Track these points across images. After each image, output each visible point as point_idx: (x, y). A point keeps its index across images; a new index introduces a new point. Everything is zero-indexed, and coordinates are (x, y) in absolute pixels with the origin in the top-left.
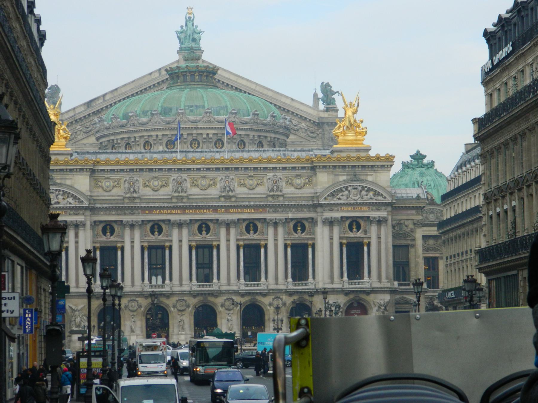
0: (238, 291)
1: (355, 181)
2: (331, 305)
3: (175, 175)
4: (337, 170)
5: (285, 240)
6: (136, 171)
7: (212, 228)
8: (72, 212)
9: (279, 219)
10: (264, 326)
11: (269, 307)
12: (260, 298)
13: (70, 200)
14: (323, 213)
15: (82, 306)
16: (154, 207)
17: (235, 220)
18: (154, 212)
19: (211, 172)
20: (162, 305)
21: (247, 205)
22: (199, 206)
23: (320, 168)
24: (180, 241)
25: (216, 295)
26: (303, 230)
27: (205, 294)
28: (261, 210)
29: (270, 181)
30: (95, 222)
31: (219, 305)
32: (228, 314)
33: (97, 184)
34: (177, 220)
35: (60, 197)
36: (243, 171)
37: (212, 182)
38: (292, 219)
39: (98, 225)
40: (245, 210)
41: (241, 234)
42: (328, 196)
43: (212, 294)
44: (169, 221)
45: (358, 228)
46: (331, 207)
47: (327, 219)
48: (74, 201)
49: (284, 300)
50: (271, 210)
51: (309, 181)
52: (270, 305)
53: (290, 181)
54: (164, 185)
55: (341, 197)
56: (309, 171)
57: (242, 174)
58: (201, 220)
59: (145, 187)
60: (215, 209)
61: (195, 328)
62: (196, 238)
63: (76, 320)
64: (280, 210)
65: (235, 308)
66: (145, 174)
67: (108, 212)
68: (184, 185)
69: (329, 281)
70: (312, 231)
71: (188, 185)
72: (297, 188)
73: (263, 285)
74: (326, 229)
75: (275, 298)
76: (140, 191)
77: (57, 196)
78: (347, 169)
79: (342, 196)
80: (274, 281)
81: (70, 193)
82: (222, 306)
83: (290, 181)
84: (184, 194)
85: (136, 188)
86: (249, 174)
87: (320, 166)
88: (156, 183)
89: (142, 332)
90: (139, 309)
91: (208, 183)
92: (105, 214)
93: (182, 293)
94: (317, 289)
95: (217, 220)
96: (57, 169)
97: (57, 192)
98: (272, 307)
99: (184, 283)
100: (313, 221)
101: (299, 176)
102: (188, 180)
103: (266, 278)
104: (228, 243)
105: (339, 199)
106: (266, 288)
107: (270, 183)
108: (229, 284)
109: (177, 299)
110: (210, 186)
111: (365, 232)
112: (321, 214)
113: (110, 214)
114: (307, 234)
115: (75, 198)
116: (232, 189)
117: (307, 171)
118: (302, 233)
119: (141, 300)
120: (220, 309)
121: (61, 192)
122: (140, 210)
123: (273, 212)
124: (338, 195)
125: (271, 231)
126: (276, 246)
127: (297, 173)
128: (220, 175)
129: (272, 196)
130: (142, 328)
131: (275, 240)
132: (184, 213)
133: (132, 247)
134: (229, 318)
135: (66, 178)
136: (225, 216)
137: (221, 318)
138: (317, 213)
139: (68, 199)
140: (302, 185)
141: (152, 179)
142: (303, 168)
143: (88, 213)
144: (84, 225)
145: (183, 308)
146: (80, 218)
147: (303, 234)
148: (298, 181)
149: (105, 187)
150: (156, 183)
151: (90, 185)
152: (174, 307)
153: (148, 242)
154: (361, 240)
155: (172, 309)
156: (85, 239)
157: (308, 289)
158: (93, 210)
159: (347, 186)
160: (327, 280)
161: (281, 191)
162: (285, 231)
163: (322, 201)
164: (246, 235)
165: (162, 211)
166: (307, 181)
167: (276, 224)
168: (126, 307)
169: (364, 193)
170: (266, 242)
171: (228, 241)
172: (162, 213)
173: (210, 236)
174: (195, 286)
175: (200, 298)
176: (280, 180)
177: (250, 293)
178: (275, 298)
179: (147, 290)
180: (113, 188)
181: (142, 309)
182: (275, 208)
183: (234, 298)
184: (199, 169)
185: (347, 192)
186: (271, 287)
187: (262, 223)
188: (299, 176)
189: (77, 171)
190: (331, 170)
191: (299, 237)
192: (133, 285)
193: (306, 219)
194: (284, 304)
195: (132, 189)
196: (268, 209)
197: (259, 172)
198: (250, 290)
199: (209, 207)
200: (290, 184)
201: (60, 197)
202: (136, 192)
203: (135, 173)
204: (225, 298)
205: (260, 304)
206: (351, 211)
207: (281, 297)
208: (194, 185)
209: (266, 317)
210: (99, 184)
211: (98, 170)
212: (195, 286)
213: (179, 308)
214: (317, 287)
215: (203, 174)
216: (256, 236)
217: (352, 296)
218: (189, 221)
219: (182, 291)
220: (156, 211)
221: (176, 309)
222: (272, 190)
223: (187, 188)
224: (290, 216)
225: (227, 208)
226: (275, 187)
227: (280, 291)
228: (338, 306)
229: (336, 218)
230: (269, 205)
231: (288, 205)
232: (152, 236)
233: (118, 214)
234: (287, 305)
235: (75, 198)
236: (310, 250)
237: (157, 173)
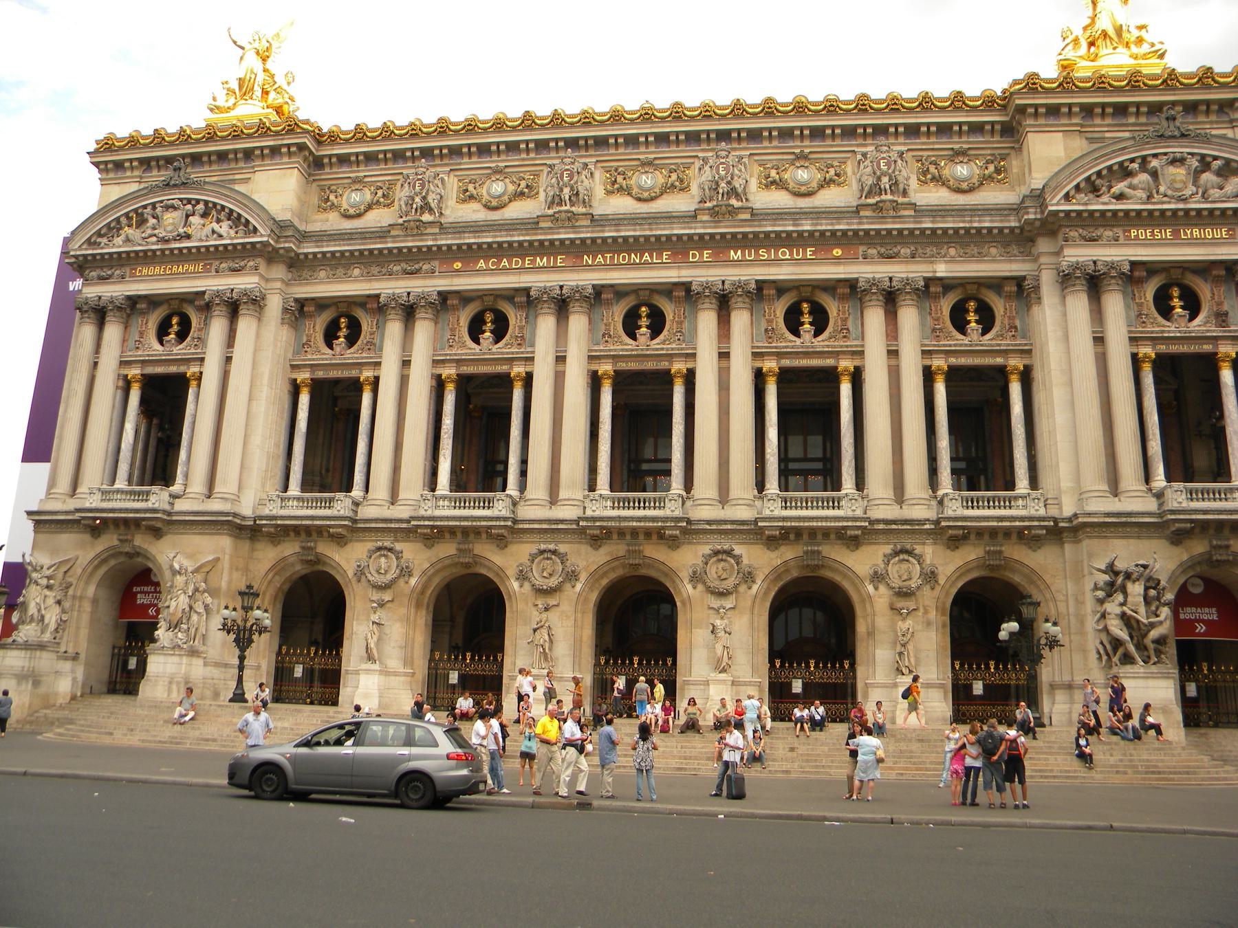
0: (756, 521)
1: (1173, 137)
2: (1128, 576)
3: (552, 159)
4: (1098, 121)
5: (926, 353)
6: (441, 156)
7: (669, 317)
8: (223, 265)
9: (902, 280)
10: (853, 665)
11: (870, 588)
12: (836, 553)
13: (224, 228)
14: (1062, 248)
15: (210, 558)
16: (480, 245)
17: (747, 283)
18: (482, 264)
19: (674, 148)
20: (483, 571)
21: (789, 234)
22: (625, 238)
23: (1036, 115)
24: (561, 359)
25: (674, 538)
26: (987, 321)
27: (634, 532)
28: (837, 252)
29: (867, 162)
30: (301, 303)
31: (685, 575)
32: (717, 611)
33: (328, 200)
34: (552, 289)
35: (195, 220)
36: (775, 143)
37: (674, 176)
38: (947, 285)
39: (311, 316)
40: (783, 253)
41: (769, 333)
42: (1077, 187)
43: (657, 534)
44: (527, 291)
45: (1193, 307)
46: (1092, 224)
47: (1076, 266)
48: (232, 232)
49: (928, 562)
50: (873, 251)
51: (998, 171)
52: (878, 578)
53: (932, 169)
54: (522, 194)
55: (1128, 191)
56: (997, 138)
57: (771, 150)
58: (635, 289)
59: (464, 201)
60: (680, 247)
61: (597, 656)
62: (614, 348)
63: (173, 604)
64: (905, 251)
65: (743, 588)
66: (466, 162)
67: (340, 271)
68: (584, 184)
69: (1106, 487)
70: (1018, 323)
71: (599, 191)
72: (959, 191)
73: (848, 506)
74: (1079, 304)
75: (896, 553)
76: (447, 212)
77: (187, 216)
78: (1132, 120)
79: (1131, 187)
80: (890, 493)
81: (223, 207)
82: (696, 578)
83: (932, 169)
84: (581, 209)
85: (431, 198)
86: (797, 151)
87: (1036, 107)
88: (497, 188)
89: (408, 661)
90: (401, 582)
91: (661, 180)
92: (333, 278)
93: (553, 530)
94: (1055, 520)
95: (686, 287)
96: (209, 154)
97: (189, 207)
98: (883, 589)
99: (563, 494)
100: (1022, 291)
101: (963, 153)
102: (597, 175)
103: (860, 484)
104: (724, 364)
105: (1120, 197)
106: (859, 513)
107: (869, 170)
108: (724, 497)
109: (534, 549)
110: (668, 189)
111: (1221, 318)
112: (1052, 260)
113: (347, 277)
114: (1000, 336)
115: (236, 220)
116: (740, 190)
117: (988, 138)
118: (984, 333)
119: (412, 552)
120: (686, 590)
121: (201, 207)
122: (436, 263)
123: (882, 256)
124: (1110, 187)
125: (875, 318)
126: (895, 375)
127: (956, 147)
128: (700, 155)
129: (877, 207)
130: (407, 646)
131: (889, 352)
132: (579, 267)
133: (404, 381)
134: (718, 622)
135: (234, 181)
136: (712, 272)
137: (690, 626)
138: (1035, 260)
139: (216, 226)
140: (975, 180)
141: (488, 176)
142: (977, 128)
143: (279, 271)
144: (257, 302)
145: (553, 582)
146: (245, 282)
147: (988, 336)
148: (962, 170)
149: (345, 206)
150: (497, 188)
151: (302, 203)
152: (522, 577)
153: (459, 362)
154: (1207, 348)
155: (516, 585)
156: (256, 350)
157: (1022, 519)
158: (297, 264)
159: (1144, 158)
160: (1095, 481)
161: (905, 193)
162: (922, 324)
163: (1056, 204)
164: (785, 340)
165: (505, 262)
166: (991, 168)
167: (890, 299)
168: (360, 573)
169: (1207, 177)
170: (857, 363)
171: (724, 356)
172: (504, 268)
173: (663, 343)
174: (603, 506)
175: (616, 548)
176: (899, 162)
177: (798, 532)
178: (896, 553)
179: (429, 513)
180: (369, 207)
181: (413, 581)
182: (886, 243)
183: (738, 550)
184: (632, 141)
185: (1144, 177)
186: (878, 513)
187: (842, 298)
188: (963, 153)
189: (263, 156)
190: (1075, 121)
191: (975, 346)
192: (394, 499)
193: (996, 284)
194: (930, 577)
195: (417, 199)
196: (861, 249)
197: (829, 142)
198: (799, 519)
199: (657, 244)
200: (933, 179)
201: (195, 220)
202: (431, 210)
203: (438, 162)
204: (707, 550)
205: (838, 578)
206: (1163, 243)
207: (918, 549)
208: (616, 188)
209: (861, 627)
210: (332, 197)
211: (330, 156)
212: (603, 506)
213: (539, 582)
214: (1054, 512)
215: (643, 154)
216: (821, 343)
217: (1199, 547)
218: (590, 290)
219: (549, 521)
220: (486, 263)
221: (527, 585)
222: (876, 189)
223: (590, 191)
224: (942, 270)
225: (720, 244)
226: (885, 180)
227: (912, 528)
228: (1152, 583)
229: (1112, 266)
230: (867, 232)
231: (934, 230)
232: (474, 345)
233: (369, 276)
234: (942, 580)
235: (236, 220)
236: (1015, 390)
237: (503, 157)
